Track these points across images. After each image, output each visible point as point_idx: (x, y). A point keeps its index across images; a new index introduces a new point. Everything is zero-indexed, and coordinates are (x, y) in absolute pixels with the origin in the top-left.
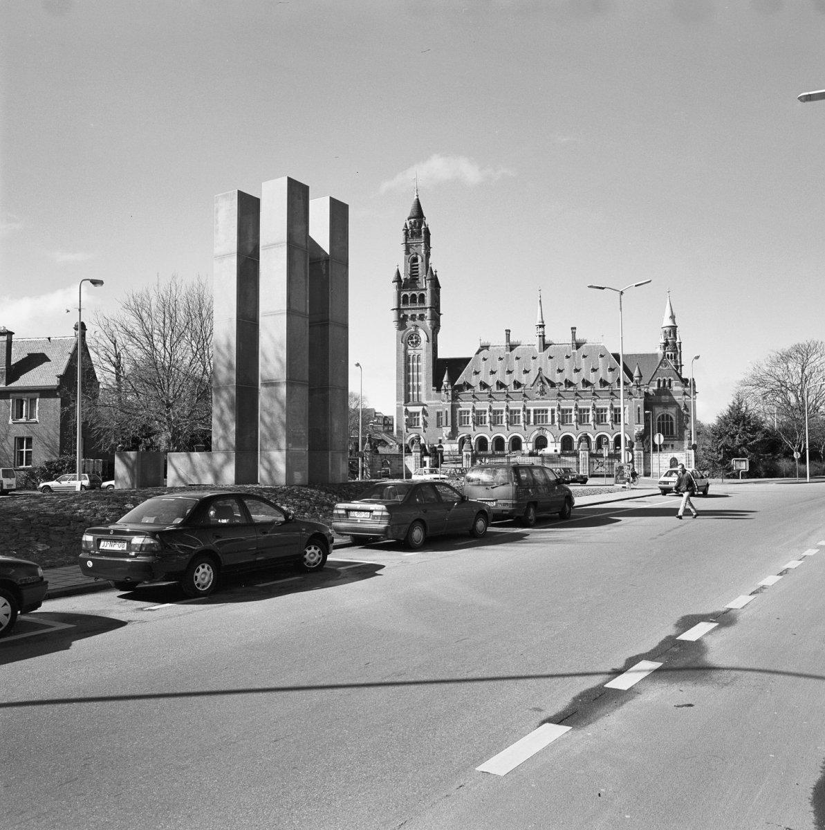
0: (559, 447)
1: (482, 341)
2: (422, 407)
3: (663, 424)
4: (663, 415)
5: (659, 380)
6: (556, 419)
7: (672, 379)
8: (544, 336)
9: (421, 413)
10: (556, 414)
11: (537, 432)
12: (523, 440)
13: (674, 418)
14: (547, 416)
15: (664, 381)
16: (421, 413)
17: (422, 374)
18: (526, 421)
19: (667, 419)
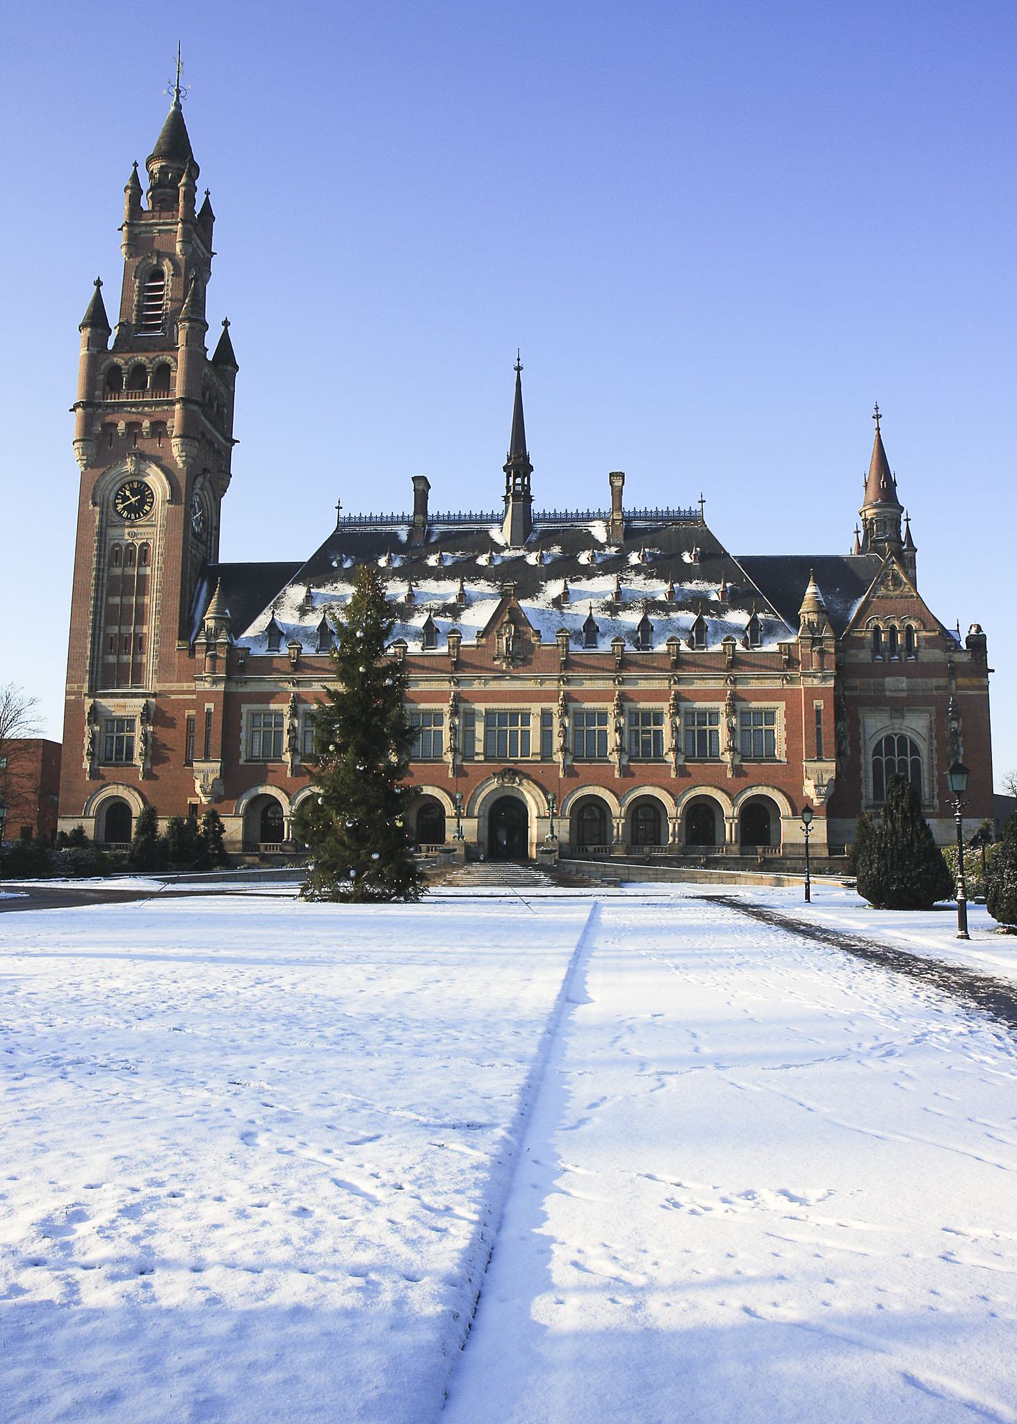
0: (563, 828)
1: (344, 513)
2: (143, 701)
3: (890, 763)
4: (889, 739)
5: (877, 628)
6: (557, 742)
7: (914, 624)
8: (528, 499)
9: (138, 722)
10: (556, 729)
11: (494, 784)
12: (449, 809)
13: (923, 747)
14: (526, 734)
15: (893, 628)
16: (138, 722)
17: (152, 601)
18: (460, 745)
19: (902, 751)
